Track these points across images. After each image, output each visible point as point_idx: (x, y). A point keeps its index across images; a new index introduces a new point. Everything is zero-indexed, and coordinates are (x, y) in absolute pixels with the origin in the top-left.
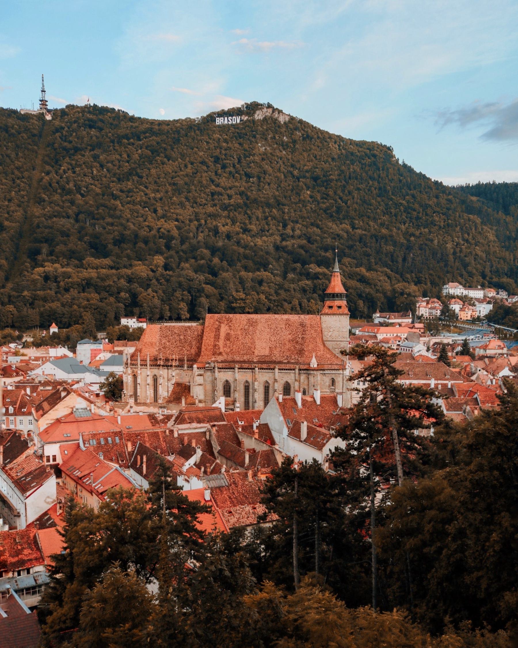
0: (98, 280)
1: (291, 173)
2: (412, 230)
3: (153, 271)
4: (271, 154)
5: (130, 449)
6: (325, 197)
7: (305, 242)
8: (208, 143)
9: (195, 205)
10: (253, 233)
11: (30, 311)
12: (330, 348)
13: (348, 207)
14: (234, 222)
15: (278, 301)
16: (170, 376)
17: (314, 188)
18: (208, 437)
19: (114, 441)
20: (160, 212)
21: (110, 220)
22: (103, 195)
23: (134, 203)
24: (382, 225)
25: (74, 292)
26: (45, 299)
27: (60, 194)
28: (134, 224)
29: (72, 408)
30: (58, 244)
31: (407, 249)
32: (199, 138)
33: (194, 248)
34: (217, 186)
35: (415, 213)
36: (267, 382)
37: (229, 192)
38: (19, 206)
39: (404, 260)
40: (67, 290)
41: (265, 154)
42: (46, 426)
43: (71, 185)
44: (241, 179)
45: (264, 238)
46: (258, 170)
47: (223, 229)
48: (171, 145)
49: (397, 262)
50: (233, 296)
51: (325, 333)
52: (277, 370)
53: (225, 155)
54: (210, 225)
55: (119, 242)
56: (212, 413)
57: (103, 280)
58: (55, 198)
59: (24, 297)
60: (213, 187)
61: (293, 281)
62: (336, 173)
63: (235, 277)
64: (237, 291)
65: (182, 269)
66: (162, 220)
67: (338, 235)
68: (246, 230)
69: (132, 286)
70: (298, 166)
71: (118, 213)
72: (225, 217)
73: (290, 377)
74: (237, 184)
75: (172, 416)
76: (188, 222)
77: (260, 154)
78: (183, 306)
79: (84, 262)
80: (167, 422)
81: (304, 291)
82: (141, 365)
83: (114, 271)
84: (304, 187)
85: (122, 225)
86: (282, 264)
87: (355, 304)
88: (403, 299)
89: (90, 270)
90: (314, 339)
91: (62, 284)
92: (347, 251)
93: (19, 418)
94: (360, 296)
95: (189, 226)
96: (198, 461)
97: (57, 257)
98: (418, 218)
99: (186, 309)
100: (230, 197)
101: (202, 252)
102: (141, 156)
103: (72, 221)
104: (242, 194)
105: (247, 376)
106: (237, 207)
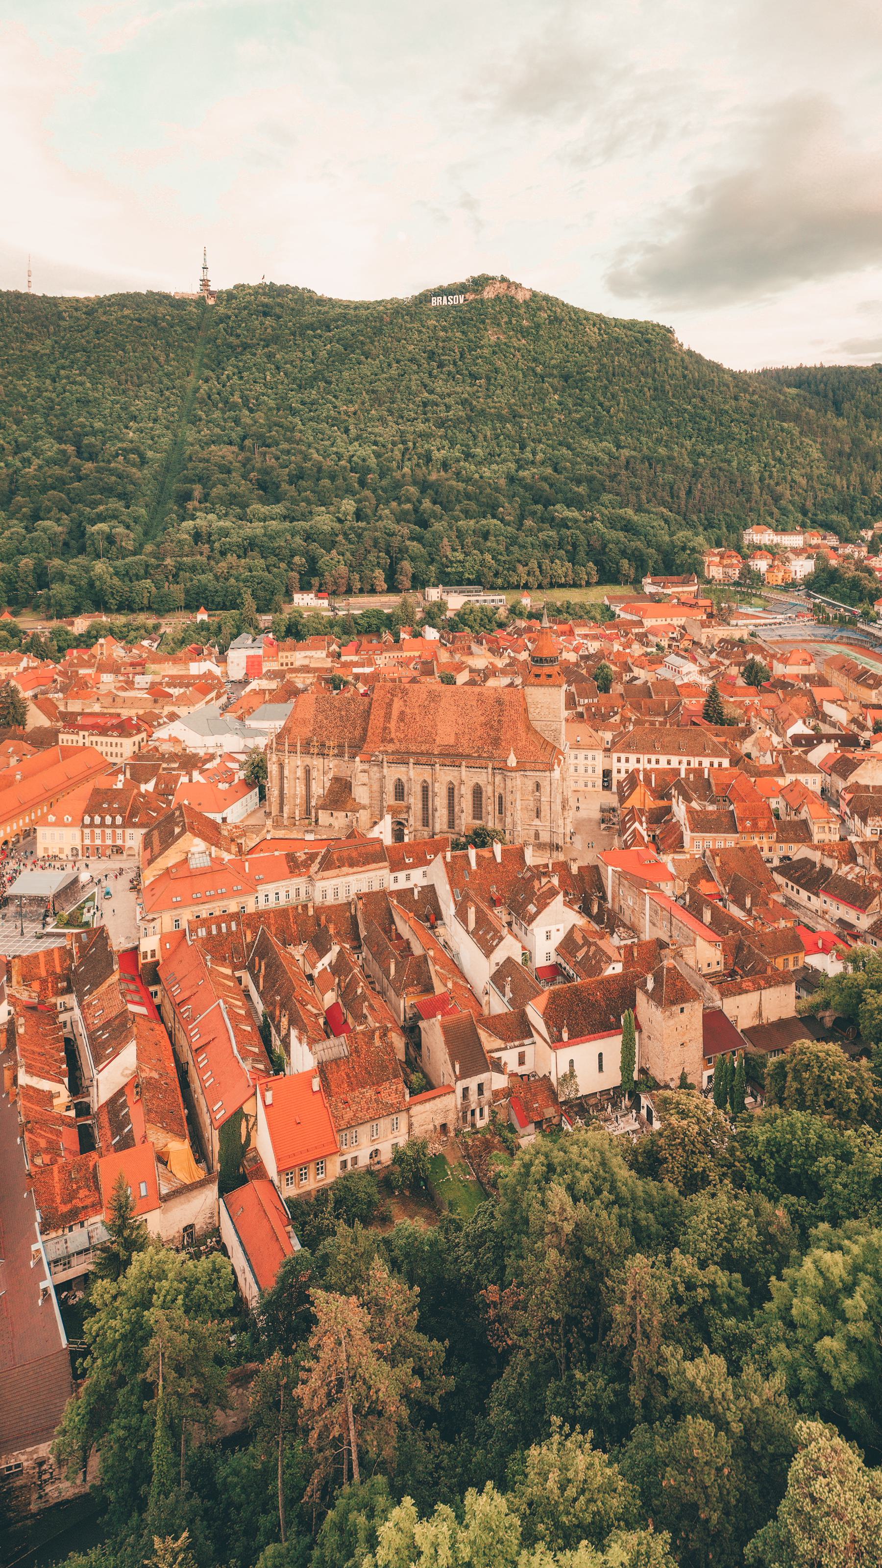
0: (265, 539)
1: (534, 371)
2: (700, 447)
3: (340, 521)
4: (505, 344)
5: (249, 939)
6: (580, 402)
7: (549, 471)
8: (420, 332)
9: (400, 421)
10: (478, 459)
11: (174, 587)
12: (538, 729)
13: (611, 417)
14: (452, 444)
15: (510, 562)
16: (326, 768)
17: (564, 391)
18: (353, 911)
19: (229, 927)
20: (353, 431)
21: (285, 446)
22: (278, 410)
23: (317, 420)
24: (659, 441)
25: (231, 558)
26: (193, 569)
27: (221, 409)
28: (318, 451)
29: (187, 853)
30: (214, 486)
31: (693, 476)
32: (409, 326)
33: (397, 485)
34: (431, 392)
35: (705, 423)
36: (451, 783)
37: (447, 400)
38: (167, 428)
39: (689, 492)
40: (223, 553)
41: (497, 345)
42: (152, 879)
43: (236, 399)
44: (463, 382)
45: (494, 467)
46: (488, 367)
47: (437, 455)
48: (370, 337)
49: (678, 498)
50: (447, 557)
51: (531, 710)
52: (463, 768)
53: (443, 348)
54: (420, 450)
55: (296, 478)
56: (370, 849)
57: (271, 538)
58: (215, 416)
59: (166, 566)
60: (426, 394)
61: (530, 532)
62: (595, 367)
63: (451, 528)
64: (454, 550)
65: (380, 518)
66: (356, 443)
67: (596, 459)
68: (468, 456)
69: (310, 547)
70: (542, 360)
71: (297, 435)
72: (441, 437)
73: (482, 777)
74: (459, 389)
75: (317, 854)
76: (390, 446)
77: (490, 346)
78: (379, 574)
79: (248, 510)
80: (310, 865)
81: (546, 546)
82: (290, 752)
83: (287, 524)
84: (551, 390)
85: (301, 452)
86: (516, 505)
87: (617, 564)
88: (685, 556)
89: (256, 524)
90: (514, 722)
91: (217, 545)
92: (607, 483)
93: (129, 831)
94: (623, 553)
95: (392, 451)
96: (334, 961)
97: (213, 504)
98: (709, 430)
99: (382, 577)
100: (448, 408)
101: (408, 491)
102: (329, 353)
103: (235, 449)
104: (464, 402)
105: (425, 773)
106: (458, 421)
